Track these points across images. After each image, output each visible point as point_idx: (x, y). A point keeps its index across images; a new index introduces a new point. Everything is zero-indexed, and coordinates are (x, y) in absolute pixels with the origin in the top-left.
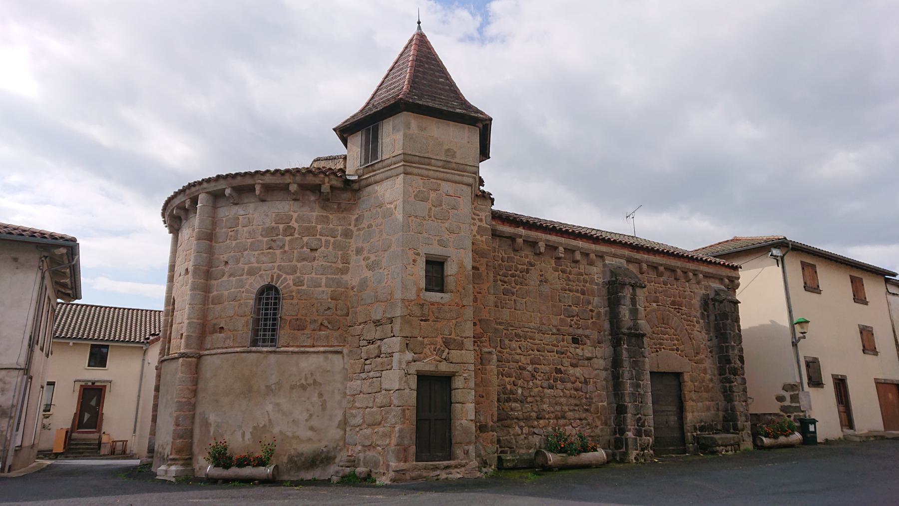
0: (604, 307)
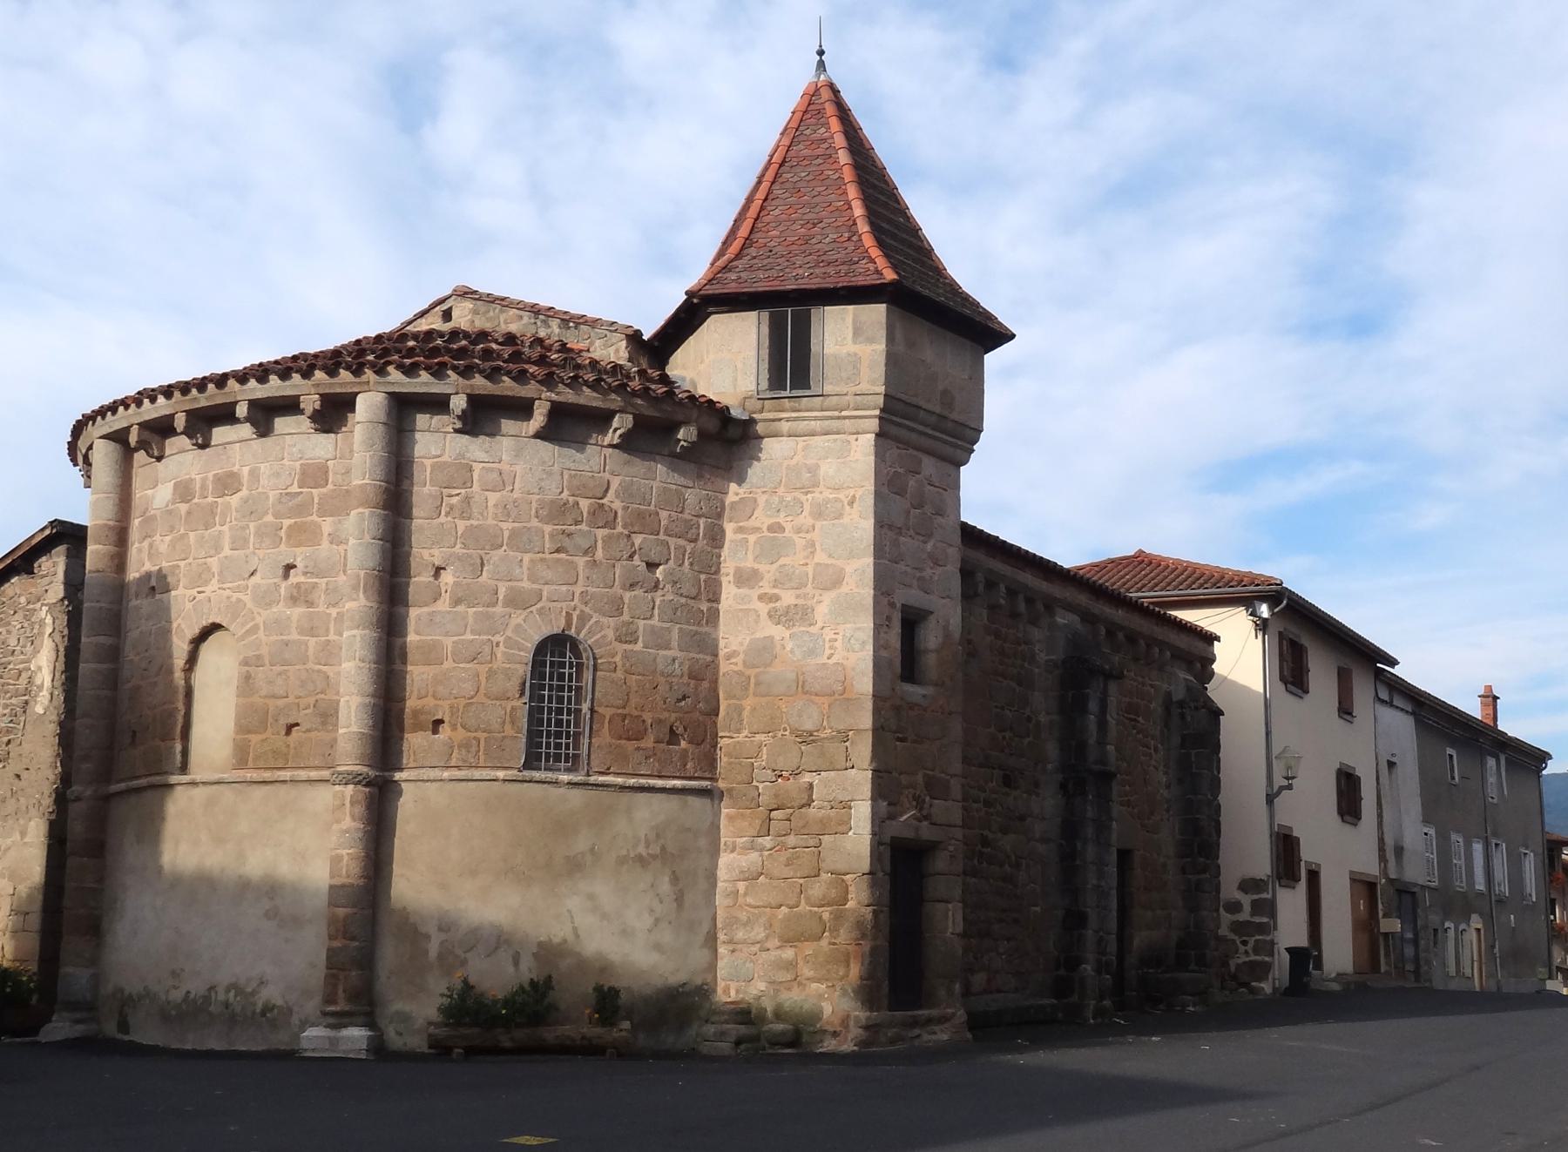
0: (1048, 713)
